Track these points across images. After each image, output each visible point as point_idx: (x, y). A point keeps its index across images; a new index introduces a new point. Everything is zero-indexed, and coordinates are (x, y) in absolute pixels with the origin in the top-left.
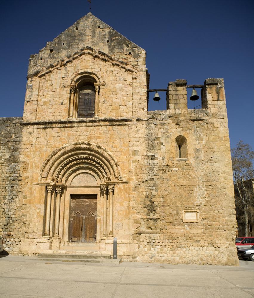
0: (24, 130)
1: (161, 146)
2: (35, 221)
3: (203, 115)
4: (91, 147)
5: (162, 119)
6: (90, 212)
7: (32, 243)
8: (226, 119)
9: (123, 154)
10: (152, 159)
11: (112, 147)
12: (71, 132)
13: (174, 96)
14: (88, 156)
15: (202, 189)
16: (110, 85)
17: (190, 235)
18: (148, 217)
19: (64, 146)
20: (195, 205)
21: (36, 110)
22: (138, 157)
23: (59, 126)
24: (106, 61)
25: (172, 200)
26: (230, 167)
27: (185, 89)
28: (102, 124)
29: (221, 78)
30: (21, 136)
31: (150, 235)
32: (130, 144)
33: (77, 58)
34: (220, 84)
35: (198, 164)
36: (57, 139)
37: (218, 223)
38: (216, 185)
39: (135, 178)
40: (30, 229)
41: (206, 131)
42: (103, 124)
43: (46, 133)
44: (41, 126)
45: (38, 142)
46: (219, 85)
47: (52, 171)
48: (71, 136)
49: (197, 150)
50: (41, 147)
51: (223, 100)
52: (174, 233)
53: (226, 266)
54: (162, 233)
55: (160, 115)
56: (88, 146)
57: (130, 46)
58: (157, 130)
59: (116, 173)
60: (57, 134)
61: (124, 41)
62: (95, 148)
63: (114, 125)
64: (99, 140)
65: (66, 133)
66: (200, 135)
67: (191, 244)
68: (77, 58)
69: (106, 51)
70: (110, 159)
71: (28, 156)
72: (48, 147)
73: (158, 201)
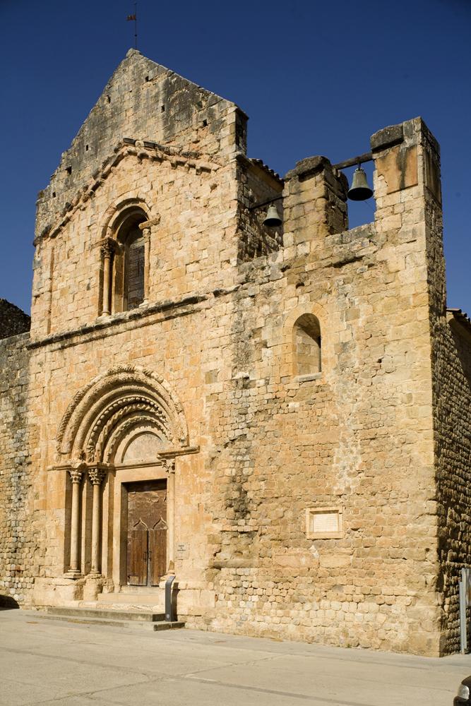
0: (31, 360)
1: (264, 350)
2: (53, 542)
3: (362, 244)
5: (266, 279)
7: (53, 589)
8: (421, 243)
10: (245, 387)
12: (102, 349)
13: (294, 209)
15: (352, 452)
16: (168, 218)
17: (321, 571)
18: (235, 528)
19: (91, 384)
20: (334, 493)
21: (50, 312)
22: (217, 387)
23: (83, 338)
24: (160, 160)
25: (282, 483)
26: (426, 382)
27: (320, 182)
28: (152, 318)
29: (414, 118)
30: (27, 374)
31: (239, 571)
33: (110, 171)
34: (411, 135)
35: (345, 383)
37: (389, 539)
38: (387, 435)
39: (210, 437)
40: (47, 558)
41: (367, 290)
42: (154, 319)
44: (57, 345)
46: (408, 142)
47: (78, 438)
49: (344, 347)
51: (417, 185)
52: (287, 566)
53: (405, 655)
54: (262, 565)
55: (263, 268)
56: (130, 376)
57: (204, 103)
58: (257, 310)
60: (82, 358)
61: (193, 96)
63: (174, 317)
65: (95, 353)
66: (352, 303)
67: (324, 594)
68: (110, 171)
69: (158, 137)
71: (39, 413)
73: (253, 489)
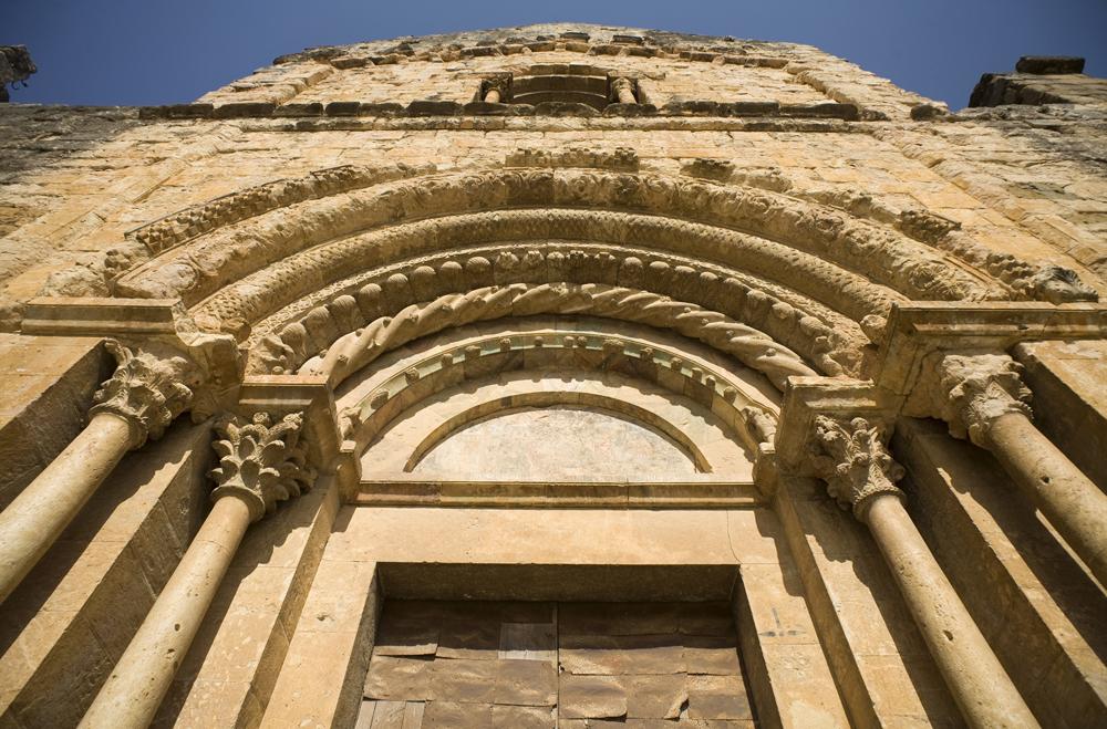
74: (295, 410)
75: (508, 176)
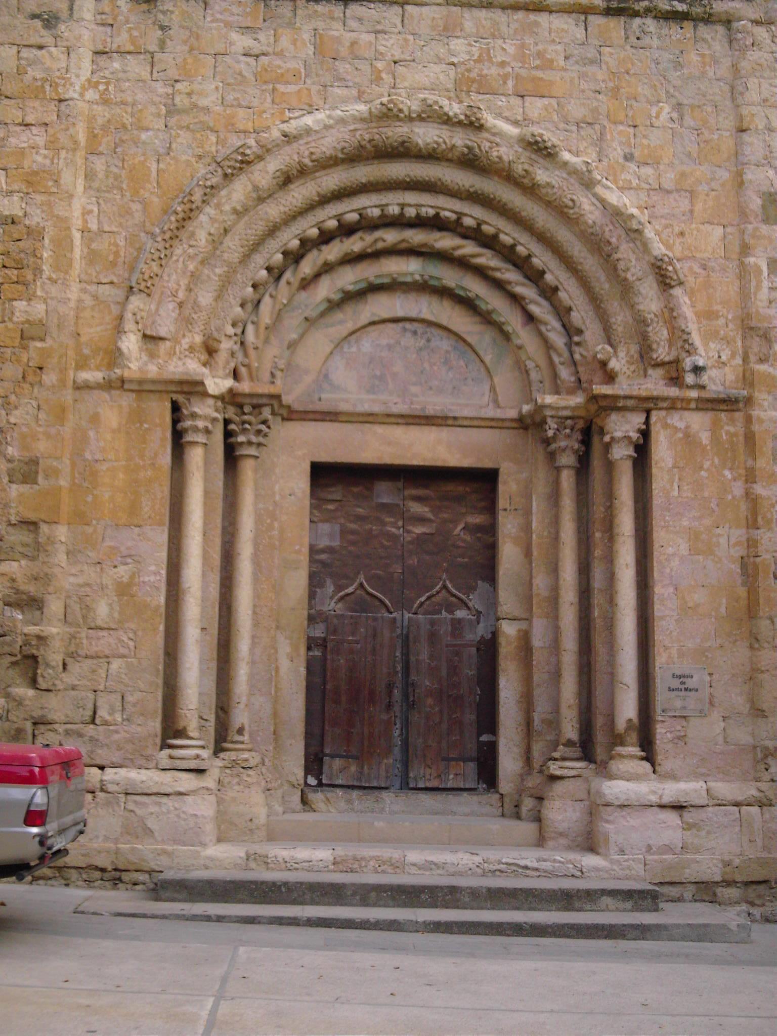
4: (486, 145)
6: (445, 587)
9: (699, 207)
11: (628, 157)
12: (336, 30)
14: (448, 207)
32: (747, 150)
36: (240, 74)
43: (162, 28)
45: (102, 87)
48: (343, 59)
50: (128, 120)
59: (660, 334)
62: (505, 153)
64: (535, 107)
70: (614, 235)
72: (181, 128)
74: (266, 405)
75: (373, 140)
